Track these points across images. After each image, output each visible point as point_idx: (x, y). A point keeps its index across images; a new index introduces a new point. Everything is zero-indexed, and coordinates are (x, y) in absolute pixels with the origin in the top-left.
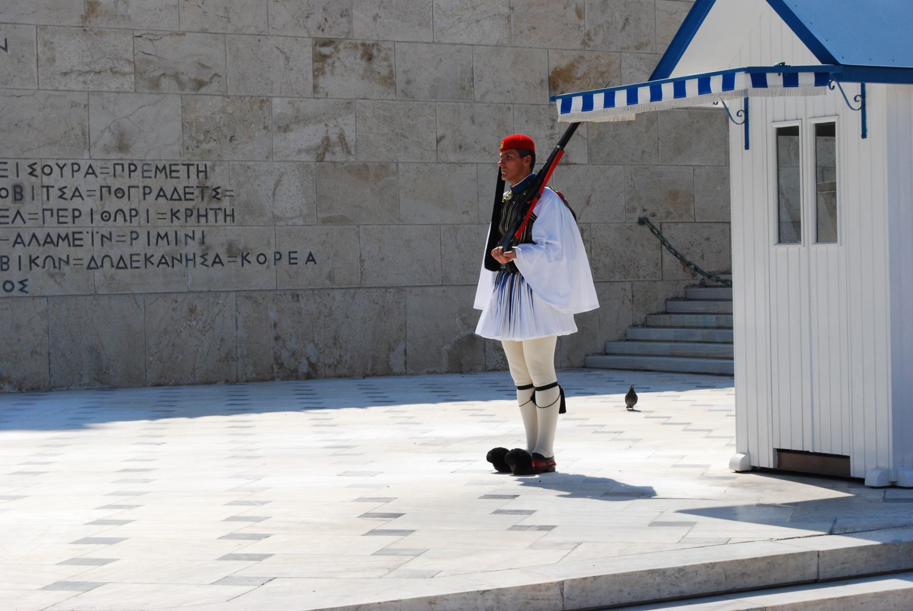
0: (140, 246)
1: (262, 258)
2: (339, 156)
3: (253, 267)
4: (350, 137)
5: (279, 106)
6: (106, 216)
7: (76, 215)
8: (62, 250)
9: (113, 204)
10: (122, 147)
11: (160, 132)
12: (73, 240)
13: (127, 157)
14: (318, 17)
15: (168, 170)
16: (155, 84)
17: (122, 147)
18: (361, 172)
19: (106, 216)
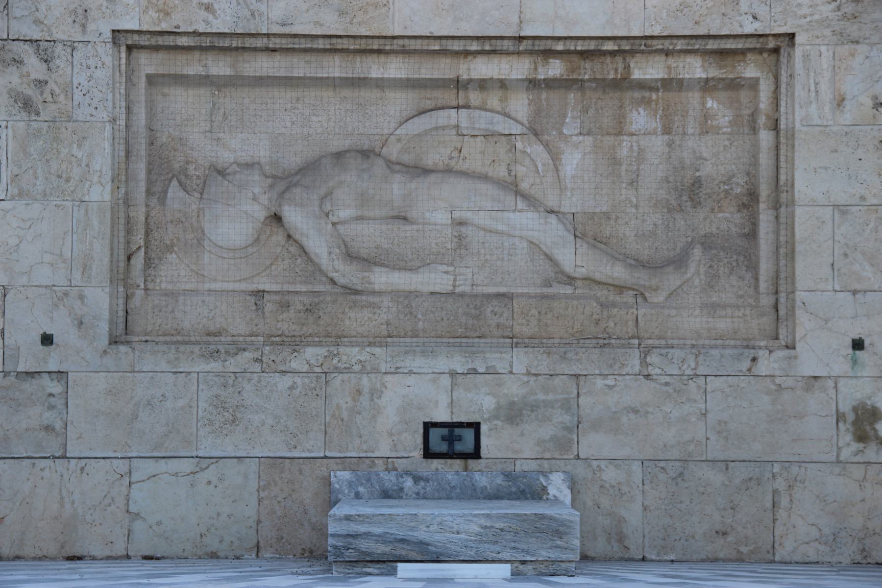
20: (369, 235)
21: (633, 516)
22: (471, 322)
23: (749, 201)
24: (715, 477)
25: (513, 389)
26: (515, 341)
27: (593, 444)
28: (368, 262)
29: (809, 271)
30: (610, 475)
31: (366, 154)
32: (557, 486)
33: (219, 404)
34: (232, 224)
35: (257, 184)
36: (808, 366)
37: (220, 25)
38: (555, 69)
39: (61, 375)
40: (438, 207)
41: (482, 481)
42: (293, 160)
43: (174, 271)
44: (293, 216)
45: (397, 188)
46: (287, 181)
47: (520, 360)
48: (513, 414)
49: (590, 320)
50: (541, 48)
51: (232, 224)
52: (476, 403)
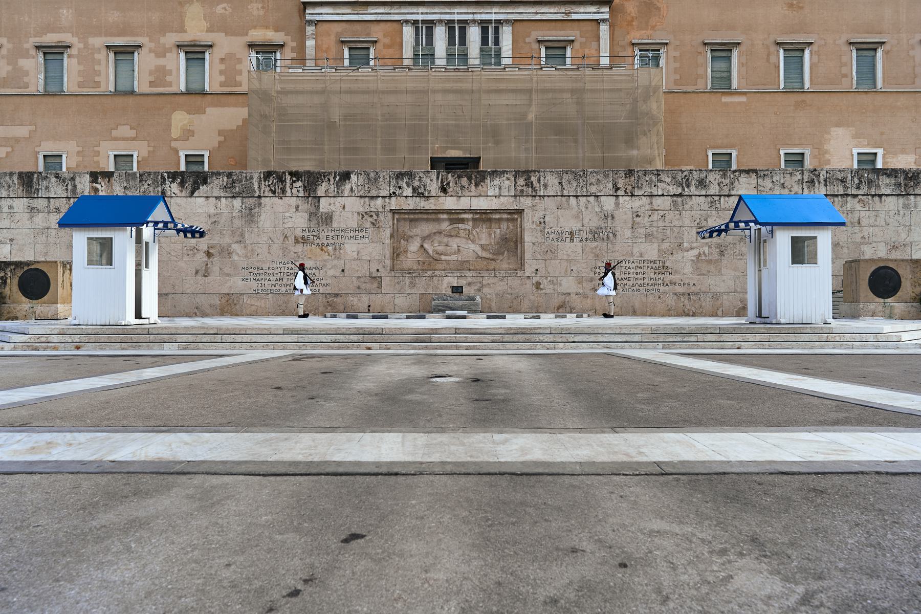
0: (646, 281)
1: (680, 285)
2: (703, 257)
3: (677, 287)
4: (707, 252)
5: (686, 245)
6: (637, 273)
7: (629, 273)
8: (625, 282)
9: (638, 271)
10: (641, 256)
11: (651, 251)
12: (628, 279)
13: (642, 259)
14: (698, 221)
15: (654, 262)
16: (651, 241)
17: (641, 256)
18: (710, 262)
19: (637, 273)
20: (440, 249)
21: (493, 304)
22: (461, 267)
23: (516, 242)
24: (509, 297)
25: (470, 280)
26: (470, 270)
27: (485, 290)
28: (441, 254)
29: (527, 256)
30: (489, 296)
31: (440, 233)
32: (478, 299)
33: (411, 283)
34: (414, 246)
35: (419, 239)
36: (527, 274)
37: (411, 208)
38: (478, 216)
39: (381, 277)
40: (454, 243)
41: (463, 297)
42: (426, 233)
43: (402, 257)
44: (426, 245)
45: (446, 239)
46: (424, 239)
47: (471, 274)
48: (469, 284)
49: (485, 264)
50: (475, 212)
51: (414, 246)
52: (462, 282)
